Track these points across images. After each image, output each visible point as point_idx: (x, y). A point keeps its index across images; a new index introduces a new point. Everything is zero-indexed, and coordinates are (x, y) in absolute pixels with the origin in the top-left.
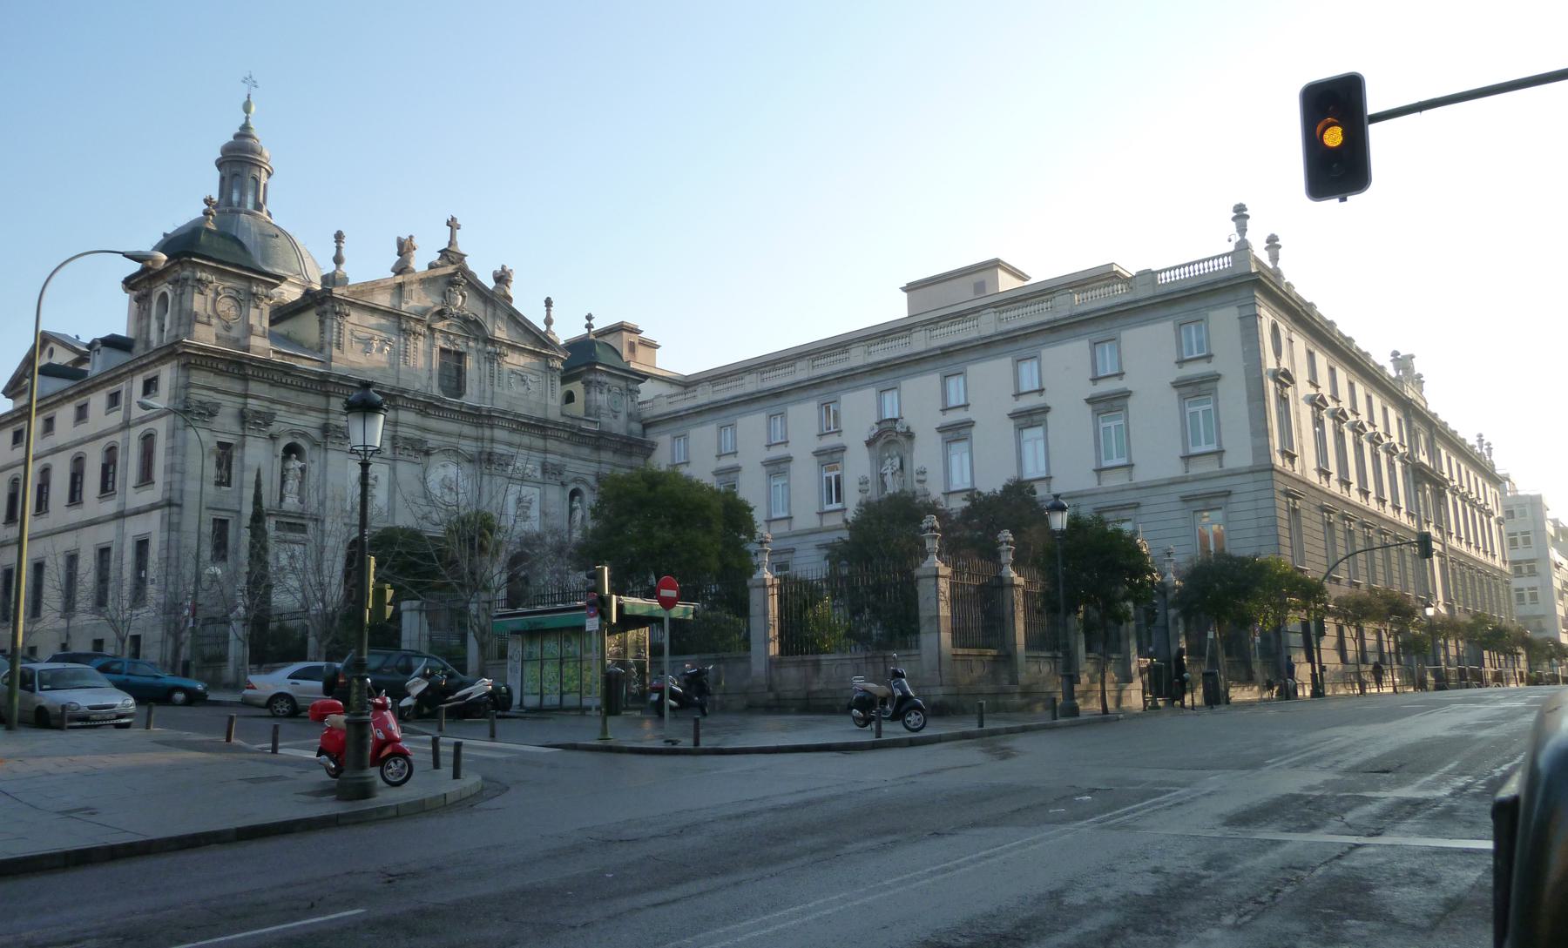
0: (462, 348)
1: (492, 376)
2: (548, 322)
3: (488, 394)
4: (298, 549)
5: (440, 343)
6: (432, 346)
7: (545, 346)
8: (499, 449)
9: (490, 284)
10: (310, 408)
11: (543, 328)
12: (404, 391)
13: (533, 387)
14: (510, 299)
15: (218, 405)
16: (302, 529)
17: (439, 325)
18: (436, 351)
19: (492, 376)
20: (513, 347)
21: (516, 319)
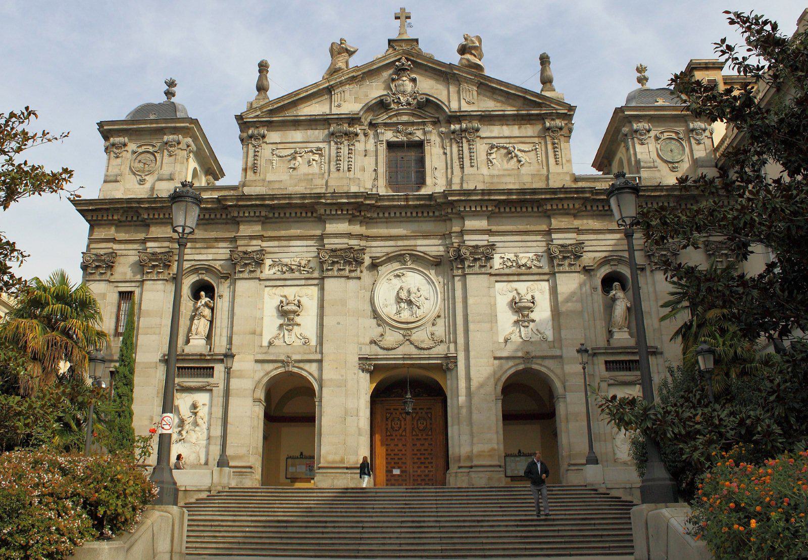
0: (419, 135)
1: (461, 158)
2: (546, 81)
3: (456, 180)
4: (202, 398)
5: (389, 135)
6: (378, 142)
7: (538, 105)
8: (472, 240)
9: (454, 59)
10: (217, 240)
11: (537, 87)
12: (319, 196)
13: (524, 157)
14: (479, 68)
15: (113, 254)
16: (209, 372)
17: (383, 118)
18: (382, 149)
19: (461, 158)
20: (488, 118)
21: (487, 86)
